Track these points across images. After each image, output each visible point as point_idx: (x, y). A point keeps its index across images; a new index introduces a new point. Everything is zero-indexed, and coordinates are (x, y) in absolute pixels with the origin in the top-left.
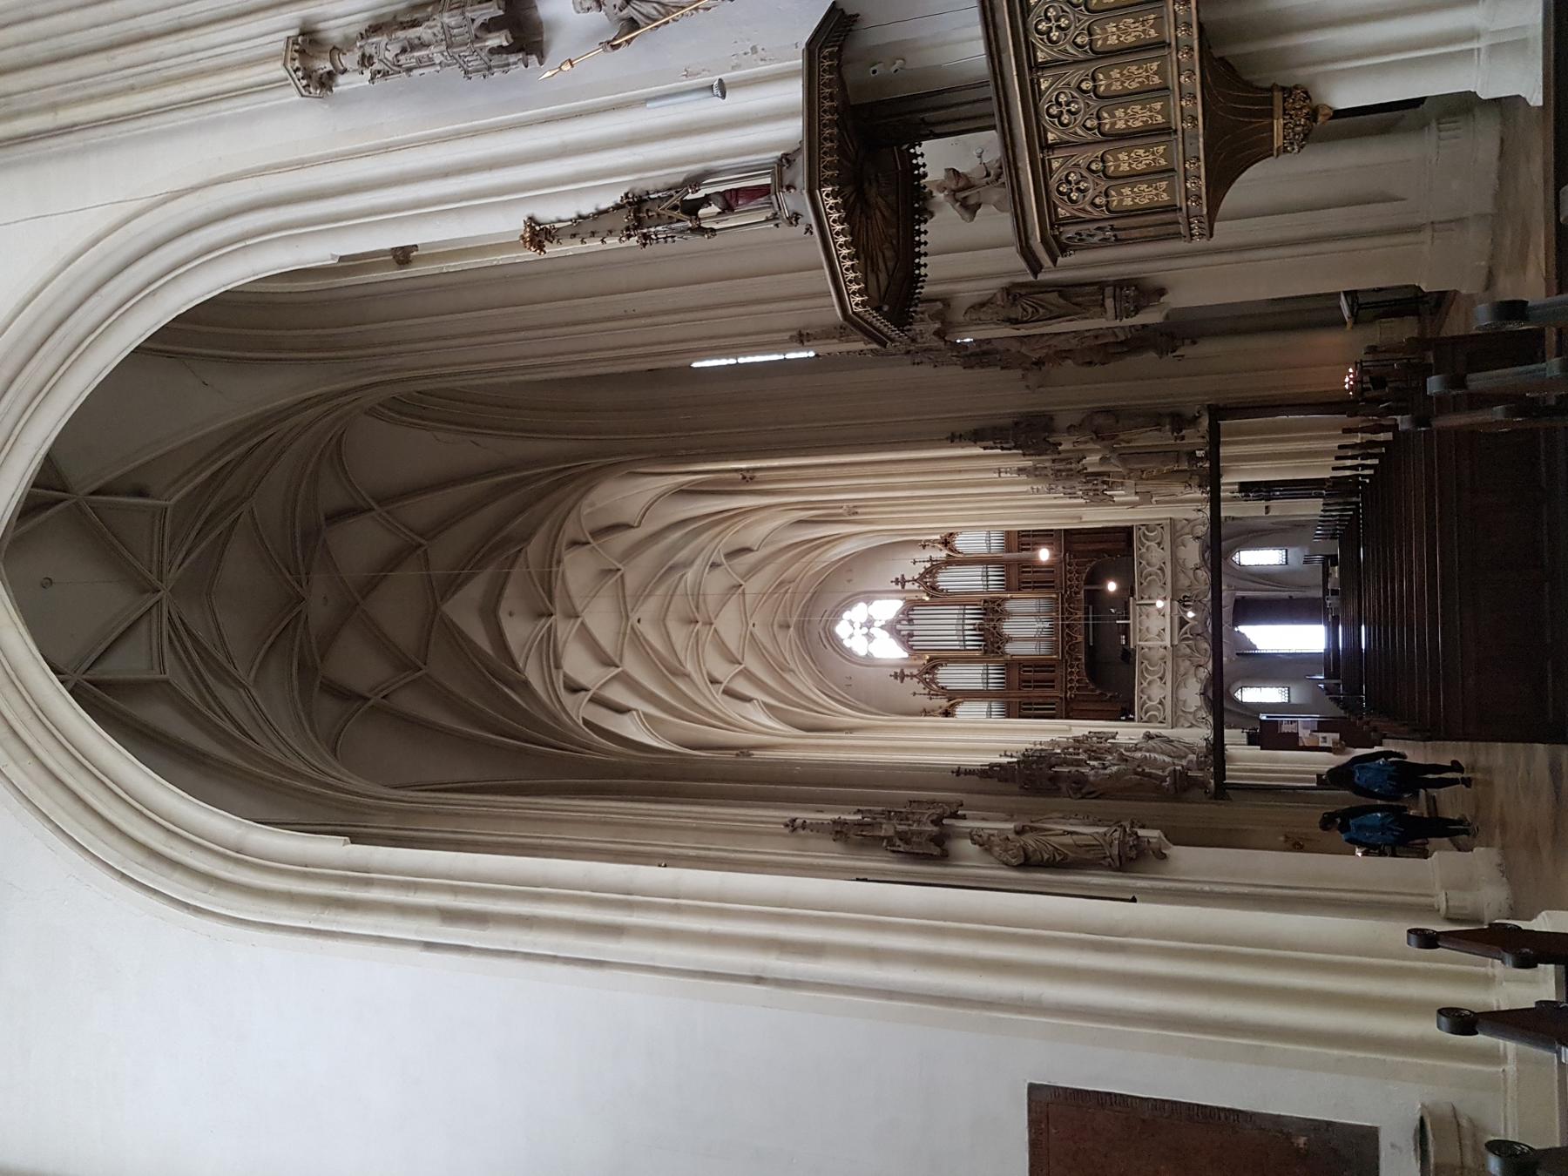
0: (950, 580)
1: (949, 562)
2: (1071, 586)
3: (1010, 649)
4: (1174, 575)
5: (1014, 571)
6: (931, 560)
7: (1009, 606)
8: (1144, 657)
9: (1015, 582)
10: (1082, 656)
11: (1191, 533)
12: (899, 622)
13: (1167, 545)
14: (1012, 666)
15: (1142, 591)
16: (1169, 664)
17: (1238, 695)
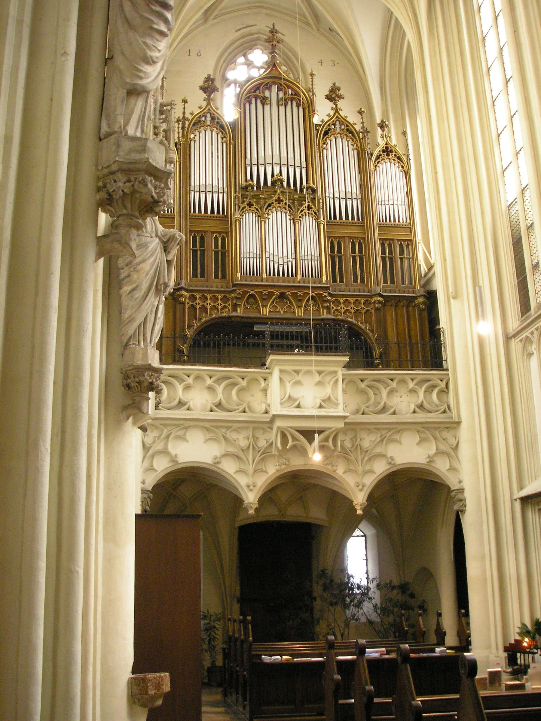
0: (339, 157)
3: (249, 219)
4: (376, 427)
5: (356, 232)
10: (240, 312)
11: (439, 453)
13: (421, 417)
15: (352, 382)
16: (242, 417)
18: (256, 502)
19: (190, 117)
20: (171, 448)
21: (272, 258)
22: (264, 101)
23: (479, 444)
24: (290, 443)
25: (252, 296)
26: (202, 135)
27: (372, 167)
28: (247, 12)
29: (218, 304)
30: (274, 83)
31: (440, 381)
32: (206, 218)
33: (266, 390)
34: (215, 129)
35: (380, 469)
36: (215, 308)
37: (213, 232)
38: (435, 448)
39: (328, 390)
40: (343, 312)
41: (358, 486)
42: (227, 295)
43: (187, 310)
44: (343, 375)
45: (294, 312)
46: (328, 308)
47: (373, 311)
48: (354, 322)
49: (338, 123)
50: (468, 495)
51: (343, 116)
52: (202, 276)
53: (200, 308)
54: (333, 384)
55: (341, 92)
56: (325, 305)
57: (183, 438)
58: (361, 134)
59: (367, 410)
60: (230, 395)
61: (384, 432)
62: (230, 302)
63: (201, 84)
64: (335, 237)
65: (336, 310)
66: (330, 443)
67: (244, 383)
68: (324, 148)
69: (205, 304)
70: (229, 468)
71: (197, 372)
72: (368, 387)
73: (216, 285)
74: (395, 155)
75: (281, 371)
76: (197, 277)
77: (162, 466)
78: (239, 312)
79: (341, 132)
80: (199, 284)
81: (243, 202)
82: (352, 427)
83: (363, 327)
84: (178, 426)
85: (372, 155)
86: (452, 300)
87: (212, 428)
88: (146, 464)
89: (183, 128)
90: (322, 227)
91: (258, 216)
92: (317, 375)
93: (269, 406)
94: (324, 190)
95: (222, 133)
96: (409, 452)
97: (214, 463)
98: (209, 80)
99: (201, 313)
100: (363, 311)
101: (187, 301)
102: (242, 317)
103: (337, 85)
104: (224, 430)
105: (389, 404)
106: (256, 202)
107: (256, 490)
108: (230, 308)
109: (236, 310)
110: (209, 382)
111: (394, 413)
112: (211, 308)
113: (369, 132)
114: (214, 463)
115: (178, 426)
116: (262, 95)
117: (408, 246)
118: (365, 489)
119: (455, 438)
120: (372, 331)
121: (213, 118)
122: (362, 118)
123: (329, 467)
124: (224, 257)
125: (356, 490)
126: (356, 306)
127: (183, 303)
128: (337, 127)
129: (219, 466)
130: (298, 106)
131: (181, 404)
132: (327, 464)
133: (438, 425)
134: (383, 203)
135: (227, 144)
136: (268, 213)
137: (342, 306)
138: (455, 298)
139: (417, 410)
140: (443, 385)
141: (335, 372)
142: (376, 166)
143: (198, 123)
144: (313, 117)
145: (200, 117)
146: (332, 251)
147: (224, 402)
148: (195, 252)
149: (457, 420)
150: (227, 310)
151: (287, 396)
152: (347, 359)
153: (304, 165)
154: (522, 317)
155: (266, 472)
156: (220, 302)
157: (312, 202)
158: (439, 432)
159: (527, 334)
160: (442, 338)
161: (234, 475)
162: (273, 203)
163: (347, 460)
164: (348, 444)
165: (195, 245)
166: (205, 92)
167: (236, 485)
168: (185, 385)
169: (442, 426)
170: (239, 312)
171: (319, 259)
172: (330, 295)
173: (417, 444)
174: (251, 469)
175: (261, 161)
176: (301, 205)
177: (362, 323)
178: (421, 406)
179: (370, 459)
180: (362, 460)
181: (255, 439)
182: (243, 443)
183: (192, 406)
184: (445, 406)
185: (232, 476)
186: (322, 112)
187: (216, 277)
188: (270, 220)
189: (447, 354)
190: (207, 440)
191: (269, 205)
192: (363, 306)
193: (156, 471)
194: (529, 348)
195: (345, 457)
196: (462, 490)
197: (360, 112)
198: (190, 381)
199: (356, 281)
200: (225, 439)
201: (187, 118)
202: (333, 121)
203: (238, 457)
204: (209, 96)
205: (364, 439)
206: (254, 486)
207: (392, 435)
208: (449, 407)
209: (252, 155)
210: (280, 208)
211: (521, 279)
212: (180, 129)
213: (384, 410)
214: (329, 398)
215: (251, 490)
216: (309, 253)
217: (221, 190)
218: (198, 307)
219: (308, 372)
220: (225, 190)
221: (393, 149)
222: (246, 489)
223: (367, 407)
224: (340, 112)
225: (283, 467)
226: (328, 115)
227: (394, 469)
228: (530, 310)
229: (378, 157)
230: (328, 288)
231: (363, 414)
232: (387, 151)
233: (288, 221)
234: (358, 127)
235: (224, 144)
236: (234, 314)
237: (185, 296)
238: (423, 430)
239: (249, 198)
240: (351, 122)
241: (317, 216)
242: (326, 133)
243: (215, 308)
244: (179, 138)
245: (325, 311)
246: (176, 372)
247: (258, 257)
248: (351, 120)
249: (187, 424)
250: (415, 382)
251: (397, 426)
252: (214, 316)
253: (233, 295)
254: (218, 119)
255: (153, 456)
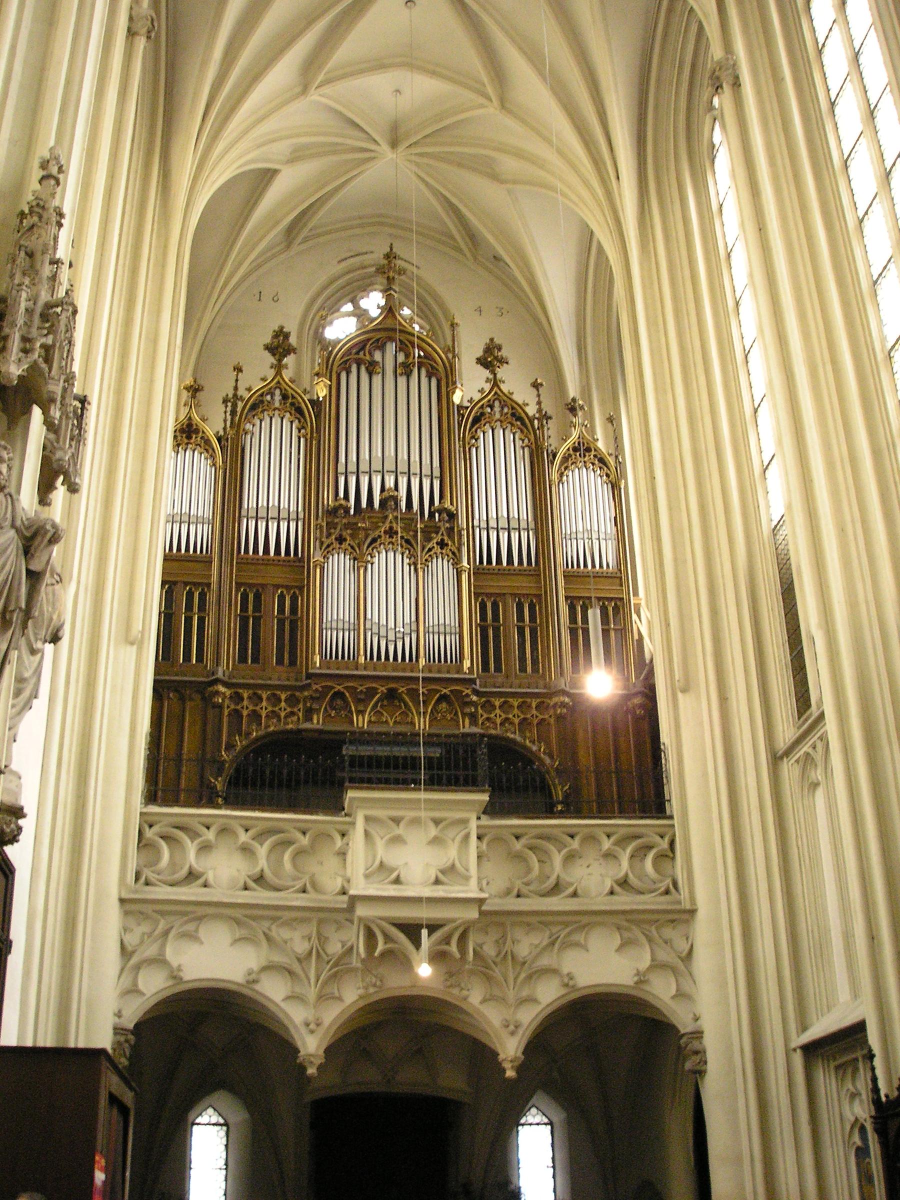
1: (538, 459)
2: (488, 706)
3: (339, 565)
5: (524, 585)
6: (545, 417)
7: (441, 568)
8: (323, 837)
9: (494, 585)
10: (317, 722)
11: (657, 966)
12: (404, 347)
13: (624, 901)
14: (296, 571)
15: (497, 839)
16: (300, 900)
17: (209, 1116)
18: (321, 1052)
19: (247, 396)
20: (169, 953)
21: (375, 630)
22: (372, 368)
23: (728, 948)
24: (381, 947)
25: (339, 695)
26: (265, 424)
27: (555, 476)
28: (358, 231)
29: (280, 709)
30: (391, 339)
31: (658, 838)
32: (266, 562)
33: (344, 854)
34: (288, 415)
35: (549, 994)
36: (274, 714)
37: (277, 587)
38: (648, 957)
39: (452, 853)
40: (498, 723)
41: (508, 1026)
42: (297, 694)
43: (225, 719)
44: (478, 827)
45: (412, 723)
46: (473, 718)
47: (552, 721)
48: (518, 738)
49: (497, 404)
50: (711, 1044)
51: (506, 392)
52: (255, 660)
53: (248, 715)
54: (461, 842)
55: (504, 353)
56: (467, 710)
57: (192, 937)
58: (536, 422)
59: (525, 890)
60: (280, 862)
61: (555, 929)
62: (301, 706)
63: (268, 339)
64: (489, 595)
65: (488, 719)
66: (454, 948)
67: (305, 841)
68: (473, 445)
69: (258, 708)
70: (274, 991)
71: (222, 821)
72: (531, 849)
73: (278, 675)
74: (595, 456)
75: (367, 819)
76: (246, 661)
77: (154, 986)
78: (315, 721)
79: (502, 418)
80: (249, 674)
81: (329, 535)
82: (493, 919)
83: (534, 748)
84: (184, 914)
85: (554, 456)
86: (680, 695)
87: (245, 920)
88: (126, 981)
89: (233, 413)
90: (465, 577)
91: (355, 559)
92: (431, 825)
93: (349, 881)
94: (470, 514)
95: (300, 422)
96: (603, 965)
97: (248, 982)
98: (281, 334)
99: (249, 724)
100: (535, 722)
101: (227, 702)
102: (320, 732)
103: (497, 341)
104: (266, 924)
105: (565, 877)
106: (351, 535)
107: (321, 1031)
108: (301, 715)
109: (308, 719)
110: (243, 837)
111: (575, 894)
112: (267, 716)
113: (550, 418)
114: (248, 982)
115: (184, 914)
116: (368, 357)
117: (616, 609)
118: (521, 1031)
119: (687, 939)
120: (551, 756)
121: (285, 397)
122: (539, 396)
123: (455, 991)
124: (294, 628)
125: (504, 1034)
126: (522, 712)
127: (220, 707)
128: (499, 410)
129: (257, 987)
130: (429, 377)
131: (192, 876)
132: (451, 986)
133: (655, 917)
134: (574, 536)
135: (306, 440)
136: (371, 554)
137: (498, 711)
138: (684, 691)
139: (617, 889)
140: (665, 844)
141: (465, 822)
142: (562, 475)
143: (257, 406)
144: (454, 393)
145: (262, 395)
146: (483, 617)
147: (268, 874)
148: (244, 621)
149: (688, 907)
150: (295, 718)
151: (377, 862)
152: (485, 797)
153: (437, 473)
154: (799, 718)
155: (340, 999)
156: (283, 704)
157: (449, 536)
158: (657, 929)
159: (806, 748)
160: (663, 762)
161: (283, 1005)
162: (380, 537)
163: (489, 979)
164: (490, 950)
165: (244, 608)
166: (274, 355)
167: (286, 1022)
168: (203, 842)
169: (663, 917)
170: (315, 721)
171: (458, 630)
172: (476, 692)
173: (617, 951)
174: (312, 993)
175: (364, 467)
176: (429, 540)
177: (533, 742)
178: (624, 883)
179: (530, 977)
180: (515, 979)
181: (322, 939)
182: (301, 947)
183: (211, 880)
184: (669, 881)
185: (277, 1005)
186: (470, 386)
187: (280, 661)
188: (376, 566)
189: (672, 790)
190: (236, 941)
191: (374, 540)
192: (534, 712)
193: (143, 994)
194: (813, 774)
195: (484, 974)
196: (698, 1034)
197: (536, 385)
198: (210, 835)
199: (523, 669)
200: (268, 938)
201: (241, 397)
202: (489, 401)
203: (291, 972)
204: (280, 361)
205: (519, 941)
206: (318, 1025)
207: (569, 934)
208: (675, 884)
209: (348, 456)
210: (393, 544)
211: (795, 653)
212: (228, 414)
213: (556, 889)
214: (453, 866)
215: (312, 1032)
216: (441, 621)
217: (293, 516)
218: (245, 713)
219: (416, 821)
220: (301, 516)
221: (592, 446)
222: (303, 1030)
223: (527, 884)
224: (502, 386)
225: (372, 990)
226: (481, 391)
227: (575, 996)
228: (809, 706)
229: (565, 459)
230: (473, 681)
231: (518, 896)
232: (583, 449)
233: (406, 568)
234: (531, 410)
235: (302, 440)
236: (307, 725)
237: (224, 694)
238: (625, 924)
239: (339, 528)
240: (520, 402)
241: (456, 559)
242: (477, 420)
243: (274, 714)
244: (225, 429)
245: (467, 721)
246: (186, 819)
247: (352, 627)
248: (518, 398)
249: (201, 911)
250: (612, 839)
251: (577, 918)
252: (272, 729)
253: (306, 693)
254: (293, 397)
255: (138, 968)
